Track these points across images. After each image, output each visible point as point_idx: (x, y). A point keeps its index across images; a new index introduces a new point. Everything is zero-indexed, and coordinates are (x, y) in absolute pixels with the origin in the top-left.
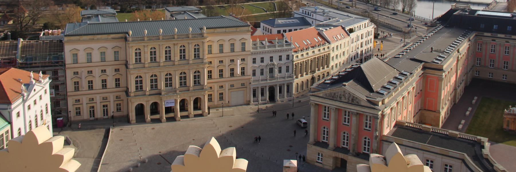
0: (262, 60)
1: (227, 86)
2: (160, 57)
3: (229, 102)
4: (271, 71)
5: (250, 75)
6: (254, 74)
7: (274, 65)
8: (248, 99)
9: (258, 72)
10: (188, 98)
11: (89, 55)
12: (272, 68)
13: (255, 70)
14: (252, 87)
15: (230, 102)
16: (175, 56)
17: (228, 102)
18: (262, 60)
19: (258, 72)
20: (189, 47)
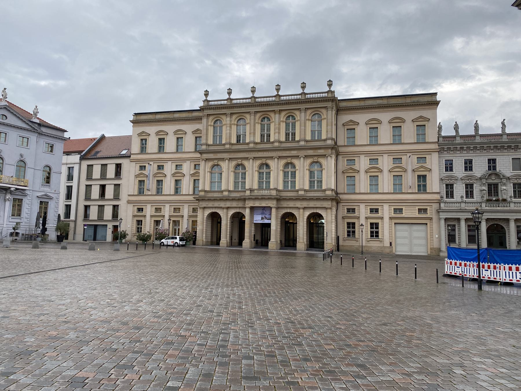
0: (468, 165)
1: (386, 212)
2: (250, 133)
3: (391, 243)
4: (493, 189)
6: (450, 193)
7: (497, 175)
8: (436, 245)
9: (459, 190)
11: (161, 141)
12: (496, 186)
13: (452, 186)
14: (443, 216)
15: (393, 244)
16: (275, 133)
17: (389, 245)
18: (468, 165)
19: (459, 190)
20: (300, 117)
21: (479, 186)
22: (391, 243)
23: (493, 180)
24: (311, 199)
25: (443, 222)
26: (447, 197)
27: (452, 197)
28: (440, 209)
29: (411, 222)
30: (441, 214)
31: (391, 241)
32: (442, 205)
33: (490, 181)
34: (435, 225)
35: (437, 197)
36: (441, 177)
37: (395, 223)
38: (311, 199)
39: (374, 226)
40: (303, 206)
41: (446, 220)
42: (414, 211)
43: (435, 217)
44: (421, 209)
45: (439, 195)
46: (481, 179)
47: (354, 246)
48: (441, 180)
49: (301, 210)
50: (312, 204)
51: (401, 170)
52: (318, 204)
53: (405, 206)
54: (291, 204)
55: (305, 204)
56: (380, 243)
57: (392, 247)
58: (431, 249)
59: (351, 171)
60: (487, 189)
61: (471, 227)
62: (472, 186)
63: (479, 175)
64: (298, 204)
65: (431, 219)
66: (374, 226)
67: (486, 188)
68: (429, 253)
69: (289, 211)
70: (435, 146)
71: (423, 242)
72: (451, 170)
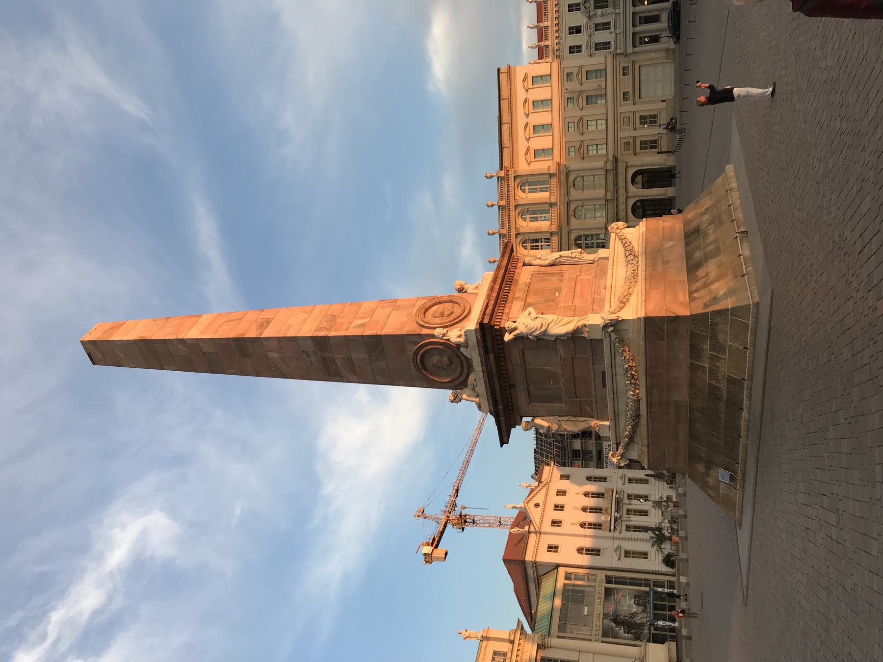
1: (626, 108)
3: (662, 101)
5: (606, 57)
6: (606, 45)
8: (663, 54)
9: (602, 36)
10: (631, 202)
13: (597, 44)
14: (630, 49)
17: (665, 103)
19: (602, 36)
21: (597, 18)
22: (662, 101)
23: (591, 5)
24: (616, 184)
25: (637, 49)
26: (609, 48)
27: (609, 43)
28: (623, 54)
29: (638, 83)
30: (628, 52)
31: (660, 101)
32: (618, 51)
33: (592, 7)
34: (641, 57)
35: (609, 59)
36: (588, 56)
37: (640, 98)
38: (616, 184)
39: (643, 120)
40: (625, 193)
41: (634, 46)
42: (626, 80)
43: (632, 58)
44: (623, 73)
45: (607, 56)
46: (590, 18)
47: (667, 141)
48: (590, 56)
49: (629, 194)
50: (621, 184)
51: (581, 97)
52: (621, 177)
53: (621, 90)
54: (622, 207)
55: (621, 191)
56: (662, 113)
57: (667, 99)
58: (666, 59)
59: (582, 150)
60: (601, 10)
61: (641, 21)
62: (596, 25)
63: (585, 19)
64: (622, 199)
65: (634, 62)
66: (643, 120)
67: (599, 11)
68: (672, 61)
69: (630, 209)
70: (555, 66)
71: (659, 68)
72: (580, 47)
